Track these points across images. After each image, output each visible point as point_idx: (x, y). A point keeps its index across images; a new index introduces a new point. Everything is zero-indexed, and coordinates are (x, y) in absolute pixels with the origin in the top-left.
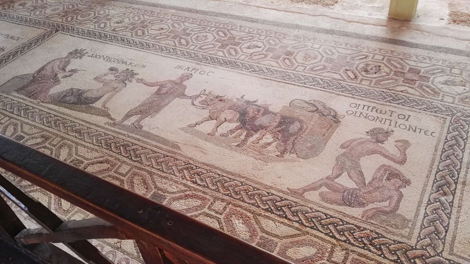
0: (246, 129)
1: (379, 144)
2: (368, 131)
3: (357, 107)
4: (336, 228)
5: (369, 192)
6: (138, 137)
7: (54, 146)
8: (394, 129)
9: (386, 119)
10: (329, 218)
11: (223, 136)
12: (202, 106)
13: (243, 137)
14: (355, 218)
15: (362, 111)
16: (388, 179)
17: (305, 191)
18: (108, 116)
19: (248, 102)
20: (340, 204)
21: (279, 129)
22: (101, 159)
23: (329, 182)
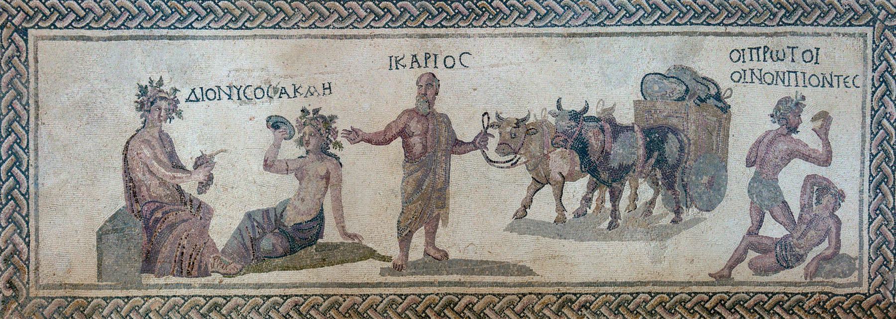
0: (604, 182)
1: (793, 135)
9: (789, 72)
11: (579, 216)
13: (608, 205)
16: (818, 202)
18: (371, 254)
21: (652, 161)
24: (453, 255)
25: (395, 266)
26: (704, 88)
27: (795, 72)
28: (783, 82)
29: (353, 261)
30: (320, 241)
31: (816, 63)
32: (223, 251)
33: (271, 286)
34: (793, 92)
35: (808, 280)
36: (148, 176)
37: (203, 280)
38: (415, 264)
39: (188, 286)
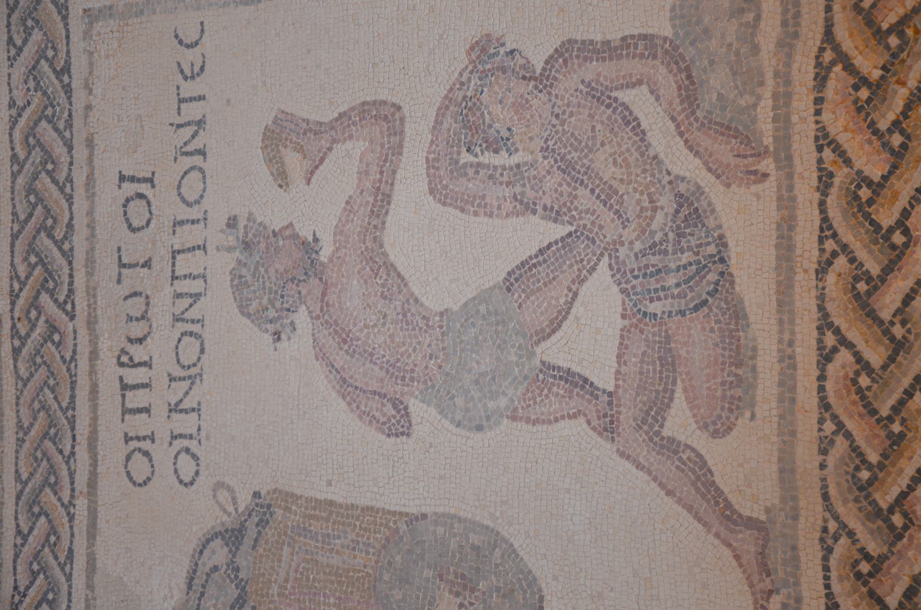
2: (268, 338)
3: (146, 445)
4: (883, 279)
5: (608, 196)
8: (218, 218)
9: (174, 278)
10: (837, 331)
14: (787, 203)
15: (160, 410)
17: (729, 516)
20: (737, 313)
23: (627, 415)
26: (211, 589)
27: (174, 253)
28: (197, 296)
31: (150, 181)
34: (219, 265)
35: (767, 165)
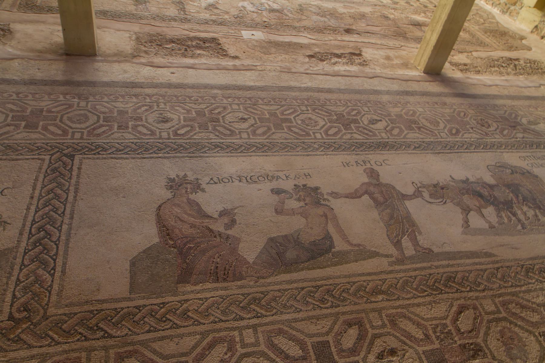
6: (444, 263)
7: (384, 326)
12: (438, 201)
18: (375, 254)
19: (463, 182)
22: (454, 309)
24: (436, 250)
25: (397, 259)
29: (364, 259)
30: (333, 250)
32: (254, 263)
33: (304, 280)
36: (179, 223)
37: (239, 283)
38: (411, 257)
39: (226, 289)
